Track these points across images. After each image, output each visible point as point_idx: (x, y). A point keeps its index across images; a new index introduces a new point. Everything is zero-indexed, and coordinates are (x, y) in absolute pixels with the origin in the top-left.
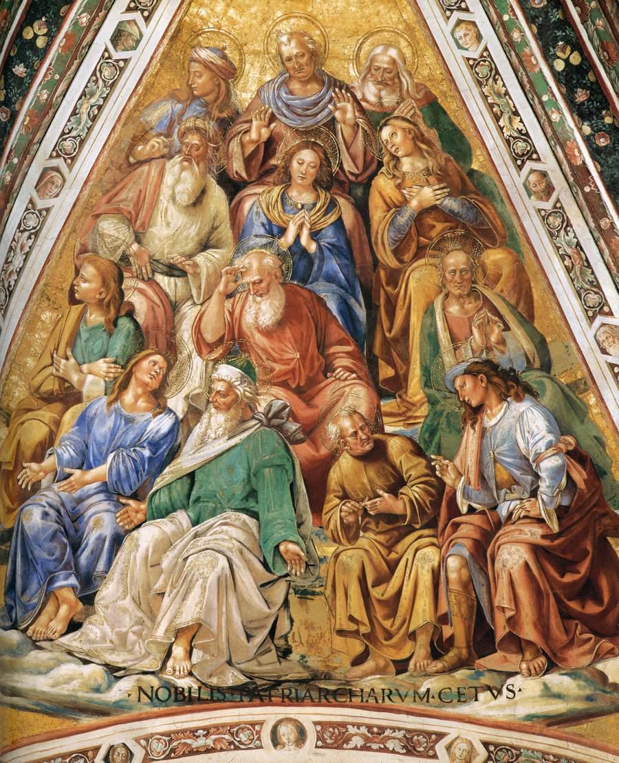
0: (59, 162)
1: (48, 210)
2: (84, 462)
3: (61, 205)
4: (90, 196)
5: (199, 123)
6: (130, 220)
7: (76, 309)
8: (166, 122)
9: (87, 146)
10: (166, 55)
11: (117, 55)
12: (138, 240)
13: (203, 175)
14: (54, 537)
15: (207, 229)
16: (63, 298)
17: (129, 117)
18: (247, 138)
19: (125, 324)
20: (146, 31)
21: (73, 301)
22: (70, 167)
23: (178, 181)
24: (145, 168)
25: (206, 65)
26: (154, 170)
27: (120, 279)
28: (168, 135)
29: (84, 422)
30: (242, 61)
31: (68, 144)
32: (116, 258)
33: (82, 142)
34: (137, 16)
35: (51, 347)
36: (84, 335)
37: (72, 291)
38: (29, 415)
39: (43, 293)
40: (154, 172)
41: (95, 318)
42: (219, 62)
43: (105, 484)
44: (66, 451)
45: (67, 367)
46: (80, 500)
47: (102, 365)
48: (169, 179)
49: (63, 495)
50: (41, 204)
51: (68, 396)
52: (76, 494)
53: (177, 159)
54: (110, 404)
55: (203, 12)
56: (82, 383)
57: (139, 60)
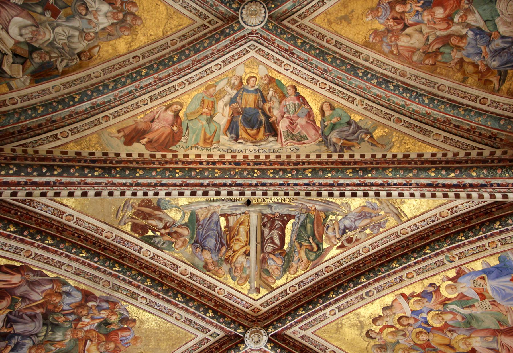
0: (398, 72)
1: (410, 74)
2: (480, 53)
3: (409, 70)
4: (406, 63)
5: (389, 38)
6: (413, 53)
7: (437, 63)
8: (388, 47)
9: (394, 66)
10: (371, 48)
11: (371, 60)
12: (419, 49)
13: (402, 35)
14: (501, 56)
15: (417, 32)
16: (434, 67)
17: (386, 55)
18: (393, 25)
19: (441, 50)
20: (365, 53)
21: (435, 64)
22: (399, 69)
23: (404, 42)
24: (400, 51)
25: (373, 39)
26: (400, 48)
27: (430, 53)
28: (391, 46)
29: (468, 56)
30: (373, 29)
31: (393, 70)
32: (423, 55)
33: (393, 67)
34: (361, 56)
35: (447, 68)
36: (444, 60)
37: (432, 65)
38: (465, 71)
39: (432, 72)
40: (401, 48)
41: (440, 58)
42: (373, 35)
43: (486, 46)
44: (476, 59)
45: (452, 63)
46: (491, 52)
47: (453, 54)
48: (403, 44)
49: (489, 56)
50: (408, 76)
51: (461, 62)
52: (489, 53)
53: (398, 42)
54: (464, 50)
55: (361, 40)
56: (457, 58)
57: (372, 54)
